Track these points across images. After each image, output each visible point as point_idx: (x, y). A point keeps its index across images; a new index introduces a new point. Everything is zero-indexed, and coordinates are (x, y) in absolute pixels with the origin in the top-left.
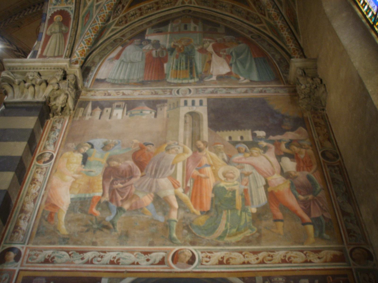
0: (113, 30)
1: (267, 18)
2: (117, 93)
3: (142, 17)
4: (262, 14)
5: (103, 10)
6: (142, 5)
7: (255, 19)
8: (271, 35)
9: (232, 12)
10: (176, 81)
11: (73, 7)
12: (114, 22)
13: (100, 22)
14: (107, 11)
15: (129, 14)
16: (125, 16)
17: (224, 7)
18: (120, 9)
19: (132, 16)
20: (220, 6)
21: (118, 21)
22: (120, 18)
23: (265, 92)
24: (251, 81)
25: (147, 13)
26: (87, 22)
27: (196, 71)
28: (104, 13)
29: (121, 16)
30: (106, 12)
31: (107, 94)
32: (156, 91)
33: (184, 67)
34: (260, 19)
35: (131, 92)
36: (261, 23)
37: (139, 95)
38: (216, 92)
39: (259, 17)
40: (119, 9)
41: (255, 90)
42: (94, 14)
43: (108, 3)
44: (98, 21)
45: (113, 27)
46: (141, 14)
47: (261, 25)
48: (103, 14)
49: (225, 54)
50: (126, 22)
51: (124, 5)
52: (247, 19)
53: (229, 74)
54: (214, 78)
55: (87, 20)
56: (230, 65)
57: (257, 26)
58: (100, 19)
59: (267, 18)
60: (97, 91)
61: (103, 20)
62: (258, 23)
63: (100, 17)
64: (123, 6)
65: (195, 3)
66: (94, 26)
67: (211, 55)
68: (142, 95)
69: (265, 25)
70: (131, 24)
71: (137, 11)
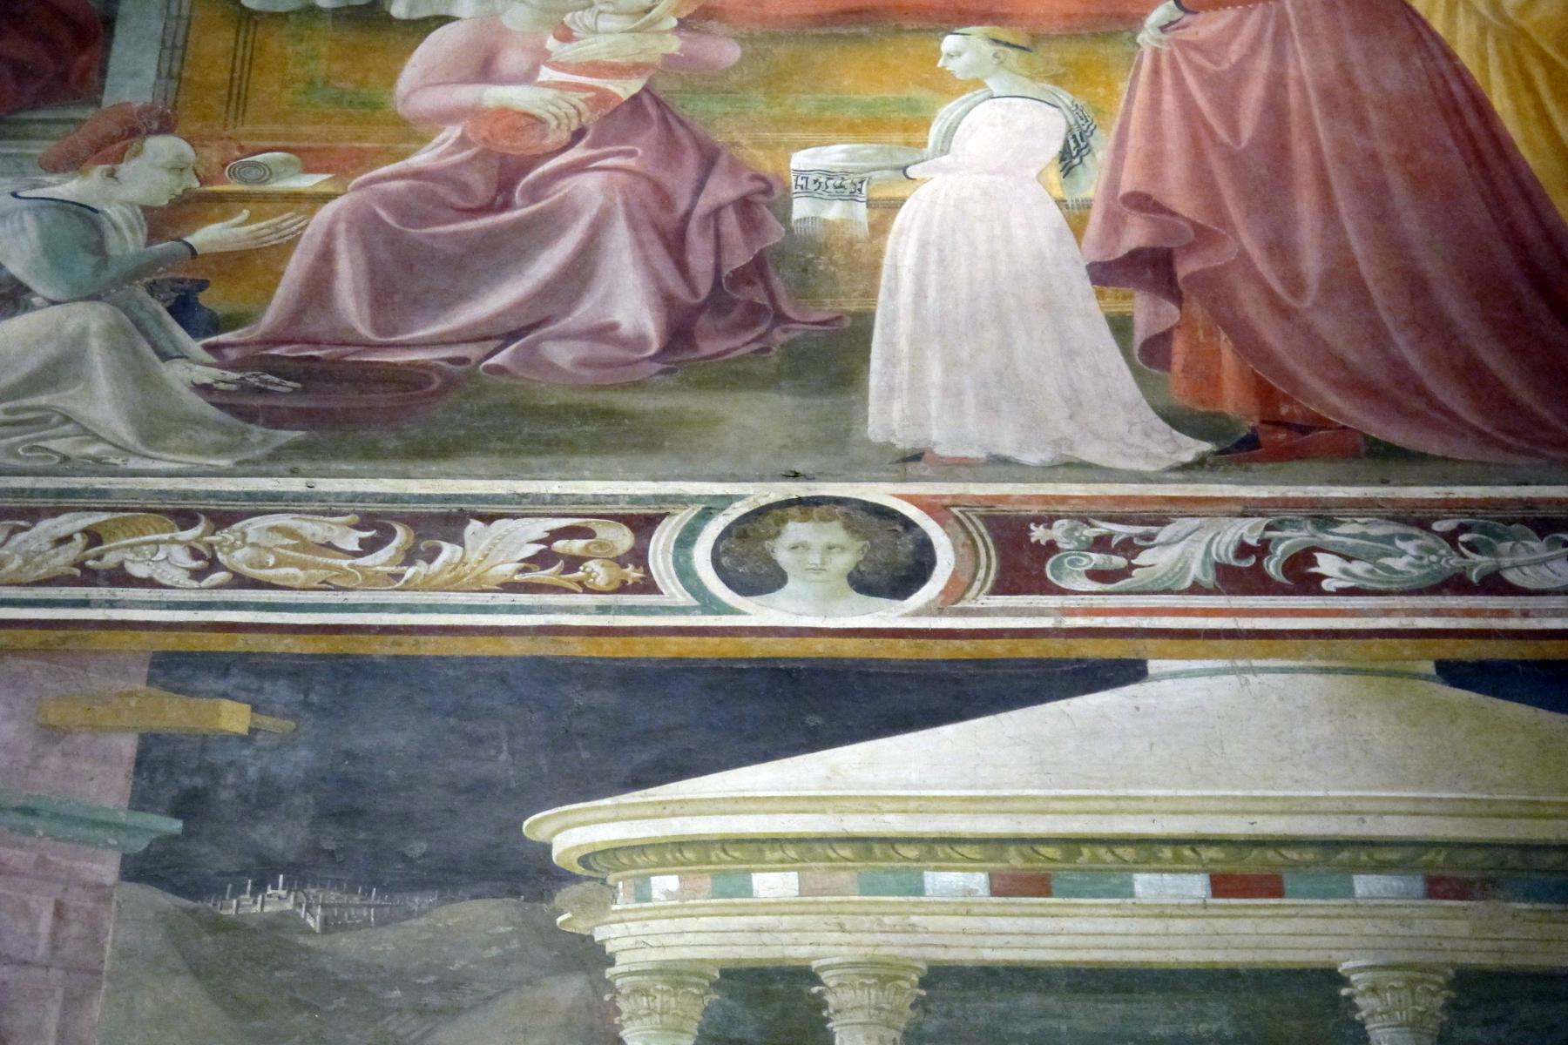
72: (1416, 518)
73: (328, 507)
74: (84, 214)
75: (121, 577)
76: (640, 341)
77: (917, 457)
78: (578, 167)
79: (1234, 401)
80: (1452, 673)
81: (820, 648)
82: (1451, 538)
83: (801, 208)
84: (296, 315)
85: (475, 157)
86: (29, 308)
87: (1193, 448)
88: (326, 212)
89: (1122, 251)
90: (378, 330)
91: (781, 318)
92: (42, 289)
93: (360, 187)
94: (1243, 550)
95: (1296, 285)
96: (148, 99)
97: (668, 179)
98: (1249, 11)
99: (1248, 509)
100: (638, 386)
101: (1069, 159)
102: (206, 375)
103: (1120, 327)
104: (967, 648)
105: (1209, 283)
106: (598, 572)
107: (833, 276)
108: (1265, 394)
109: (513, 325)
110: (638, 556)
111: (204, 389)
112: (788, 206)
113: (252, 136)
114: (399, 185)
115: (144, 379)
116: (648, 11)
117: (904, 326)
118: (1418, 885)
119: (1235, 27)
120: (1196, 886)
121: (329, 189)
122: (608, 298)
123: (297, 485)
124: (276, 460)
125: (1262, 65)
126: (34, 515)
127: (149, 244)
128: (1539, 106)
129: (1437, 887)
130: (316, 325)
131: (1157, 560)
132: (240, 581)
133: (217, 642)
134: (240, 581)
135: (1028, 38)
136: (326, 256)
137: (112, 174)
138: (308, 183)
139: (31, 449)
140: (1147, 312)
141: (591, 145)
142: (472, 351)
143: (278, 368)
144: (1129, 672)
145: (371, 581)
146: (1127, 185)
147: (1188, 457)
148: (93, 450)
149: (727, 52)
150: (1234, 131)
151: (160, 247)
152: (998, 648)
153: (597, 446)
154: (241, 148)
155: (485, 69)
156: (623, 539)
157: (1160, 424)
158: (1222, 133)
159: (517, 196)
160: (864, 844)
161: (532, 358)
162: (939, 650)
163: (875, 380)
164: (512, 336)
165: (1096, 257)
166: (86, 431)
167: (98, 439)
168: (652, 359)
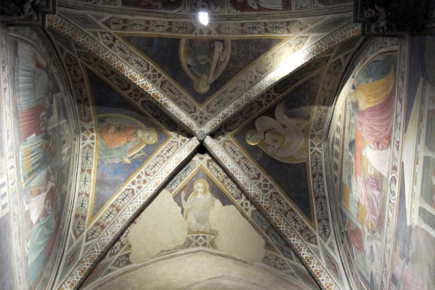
0: (62, 50)
1: (84, 244)
2: (6, 79)
3: (71, 83)
4: (88, 236)
5: (94, 43)
6: (86, 83)
7: (78, 227)
8: (65, 254)
9: (80, 194)
10: (21, 158)
11: (100, 4)
12: (73, 52)
13: (81, 40)
14: (92, 49)
15: (79, 68)
16: (77, 64)
17: (85, 184)
18: (87, 60)
19: (75, 72)
20: (85, 178)
21: (72, 56)
22: (76, 58)
23: (20, 283)
24: (27, 258)
25: (75, 88)
26: (80, 21)
27: (31, 180)
28: (91, 44)
29: (79, 60)
30: (91, 47)
31: (4, 65)
32: (11, 135)
33: (34, 162)
34: (80, 235)
35: (8, 101)
36: (77, 237)
37: (6, 113)
38: (15, 220)
39: (82, 232)
40: (89, 59)
41: (20, 270)
42: (88, 30)
43: (101, 47)
44: (82, 38)
45: (66, 50)
46: (74, 82)
47: (74, 237)
48: (90, 44)
49: (47, 206)
50: (68, 65)
51: (91, 64)
52: (77, 216)
53: (32, 225)
54: (27, 208)
55: (82, 21)
56: (38, 221)
57: (71, 231)
58: (84, 40)
59: (84, 244)
60: (6, 49)
61: (83, 43)
62: (74, 232)
63: (87, 39)
64: (90, 63)
65: (84, 145)
66: (78, 34)
67: (45, 190)
68: (6, 117)
69: (76, 243)
70: (65, 70)
71: (80, 77)
72: (395, 129)
73: (387, 229)
75: (389, 250)
80: (405, 132)
81: (399, 191)
82: (397, 127)
87: (389, 148)
94: (396, 147)
99: (394, 145)
101: (371, 148)
104: (400, 177)
105: (380, 140)
106: (393, 208)
110: (392, 203)
118: (419, 145)
120: (417, 166)
123: (385, 230)
124: (384, 230)
126: (385, 255)
129: (419, 143)
131: (396, 156)
132: (390, 240)
133: (394, 245)
134: (390, 240)
136: (372, 218)
143: (378, 227)
144: (403, 163)
145: (391, 228)
149: (362, 174)
152: (400, 174)
153: (385, 202)
155: (362, 196)
156: (391, 204)
160: (412, 196)
162: (400, 179)
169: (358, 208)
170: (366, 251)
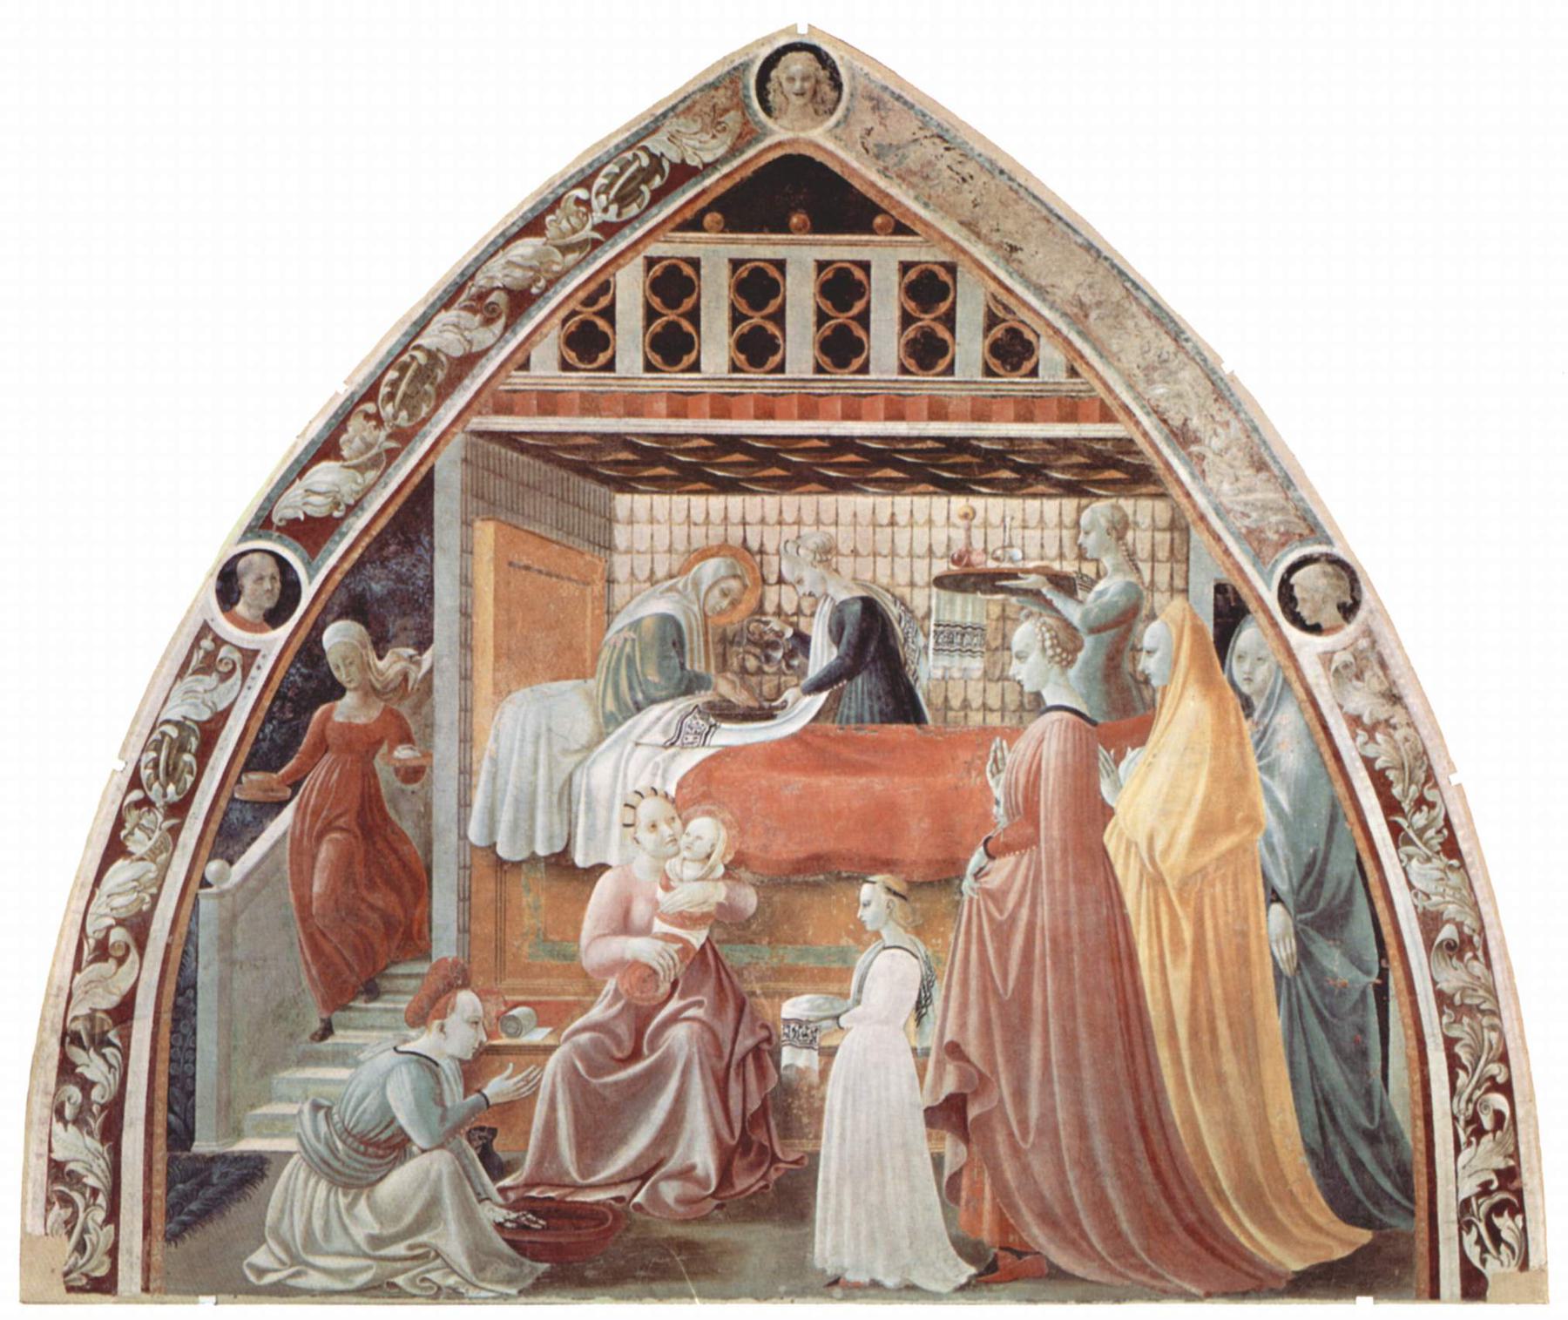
74: (428, 1064)
76: (703, 1183)
77: (836, 1282)
78: (674, 1019)
79: (987, 1233)
83: (788, 1056)
84: (539, 1163)
85: (623, 1008)
86: (412, 1156)
88: (553, 1062)
89: (942, 1097)
90: (583, 1177)
91: (775, 1159)
92: (419, 1139)
93: (568, 1038)
95: (1023, 1122)
96: (454, 954)
97: (717, 1026)
98: (1022, 855)
100: (704, 1219)
102: (500, 1215)
103: (938, 1162)
107: (799, 1119)
108: (1004, 1227)
109: (646, 1167)
111: (500, 1226)
112: (779, 1053)
113: (513, 991)
114: (584, 1037)
115: (469, 1218)
116: (709, 857)
117: (834, 1166)
119: (1017, 865)
121: (551, 1041)
122: (690, 1147)
125: (1024, 913)
127: (465, 1097)
128: (1162, 956)
130: (549, 1171)
135: (905, 885)
137: (442, 1028)
138: (539, 1036)
139: (424, 1280)
140: (954, 1152)
141: (682, 997)
142: (624, 1191)
146: (948, 1038)
147: (963, 1280)
148: (452, 1280)
150: (1006, 990)
151: (473, 1098)
154: (506, 1003)
157: (952, 1251)
158: (998, 981)
159: (645, 1050)
161: (654, 1195)
163: (819, 1214)
164: (644, 1178)
165: (928, 1101)
166: (448, 1265)
167: (454, 1272)
168: (713, 1195)
169: (533, 858)
170: (342, 1057)
